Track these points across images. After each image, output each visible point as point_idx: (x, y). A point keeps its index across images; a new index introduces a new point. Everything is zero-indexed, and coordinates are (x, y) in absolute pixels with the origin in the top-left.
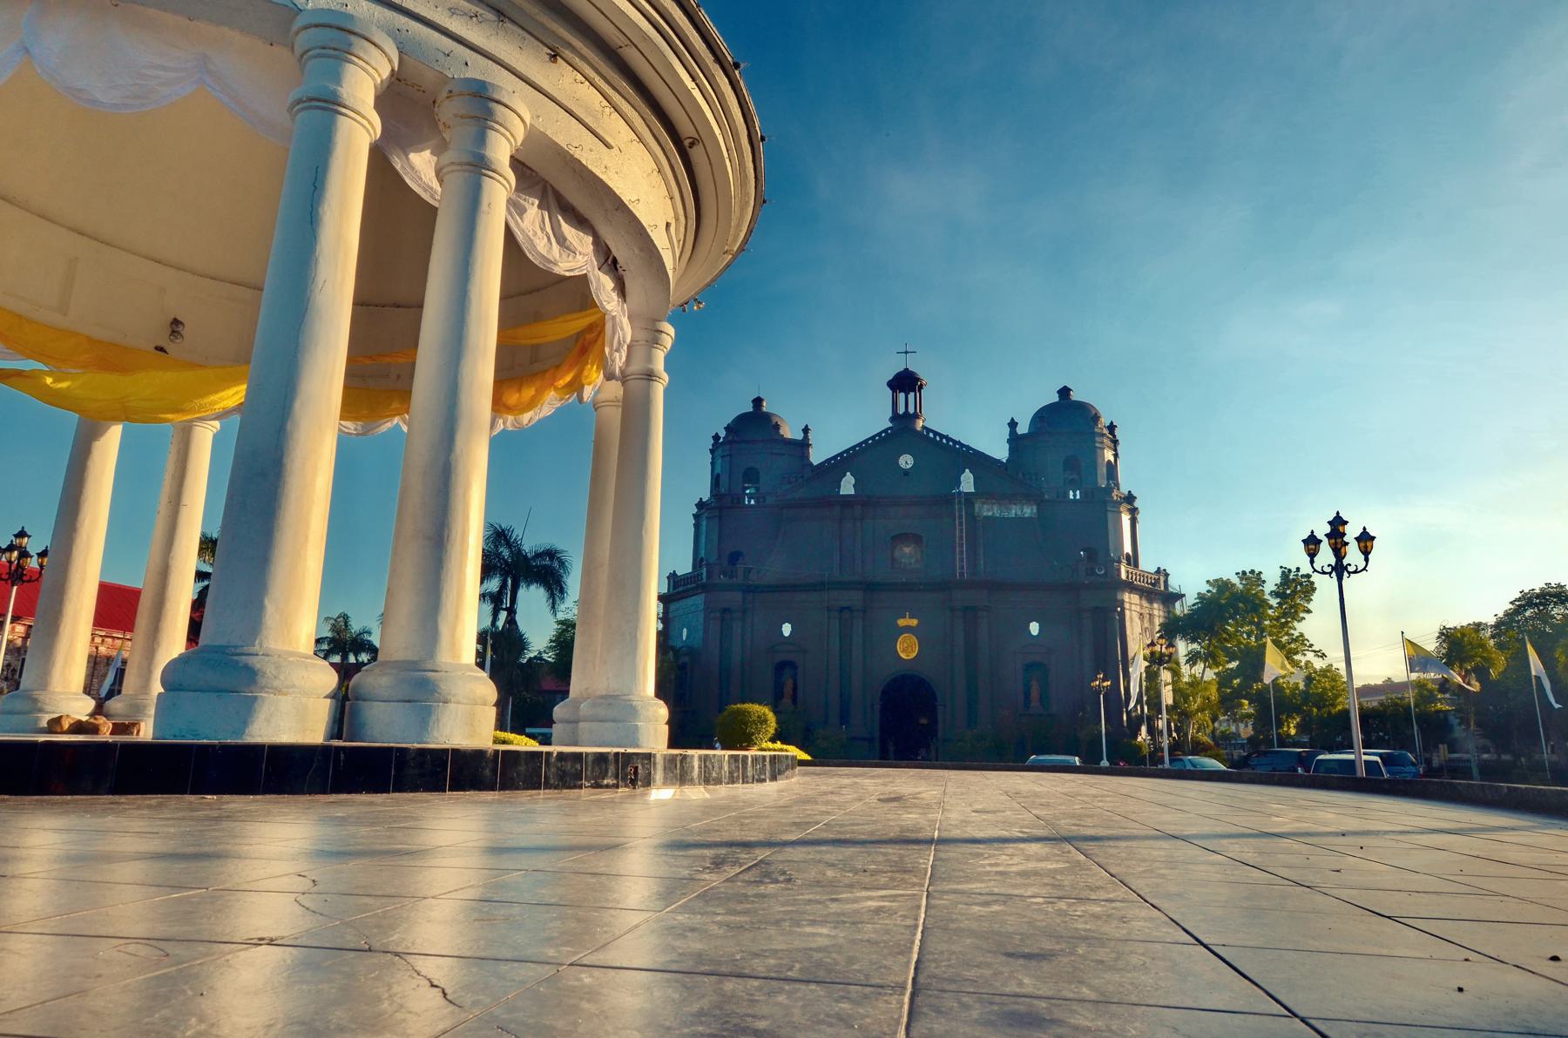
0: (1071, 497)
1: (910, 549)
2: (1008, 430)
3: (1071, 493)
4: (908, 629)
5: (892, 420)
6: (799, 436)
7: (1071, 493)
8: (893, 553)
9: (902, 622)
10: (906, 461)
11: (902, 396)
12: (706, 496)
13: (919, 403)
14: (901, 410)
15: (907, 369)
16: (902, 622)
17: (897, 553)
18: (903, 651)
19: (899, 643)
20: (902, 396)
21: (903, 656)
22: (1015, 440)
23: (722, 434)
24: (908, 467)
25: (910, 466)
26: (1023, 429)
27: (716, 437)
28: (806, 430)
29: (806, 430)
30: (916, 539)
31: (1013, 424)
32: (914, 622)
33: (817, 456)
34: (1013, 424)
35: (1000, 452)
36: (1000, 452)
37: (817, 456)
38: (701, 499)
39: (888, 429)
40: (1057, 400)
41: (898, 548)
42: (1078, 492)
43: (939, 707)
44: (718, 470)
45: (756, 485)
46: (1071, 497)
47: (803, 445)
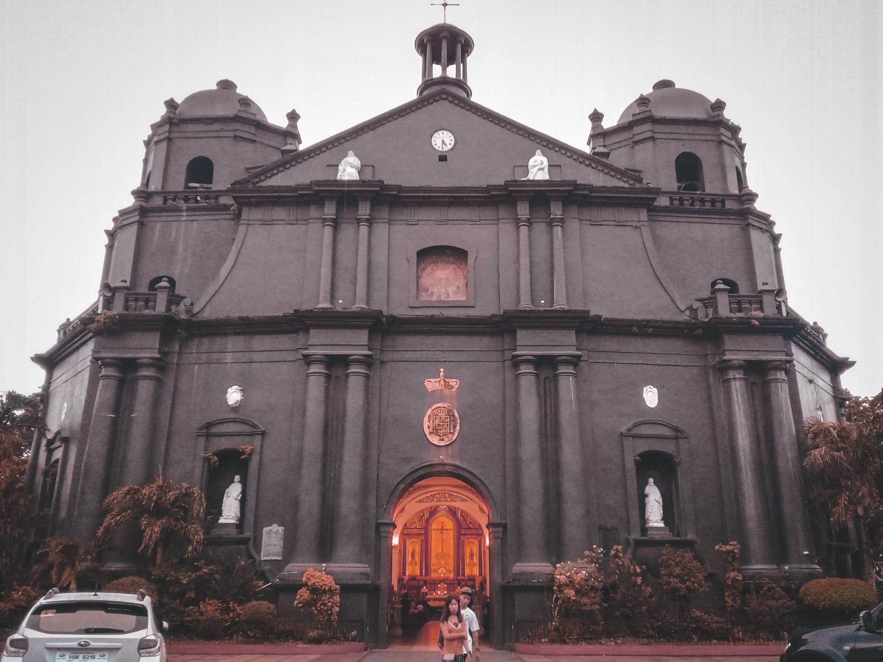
1: (447, 272)
2: (589, 125)
4: (437, 396)
5: (422, 90)
6: (283, 123)
8: (418, 278)
9: (432, 385)
10: (443, 140)
16: (432, 385)
17: (426, 281)
18: (435, 431)
19: (426, 419)
21: (435, 440)
22: (598, 135)
24: (446, 149)
25: (450, 147)
26: (609, 122)
28: (293, 117)
29: (293, 117)
30: (457, 255)
31: (596, 117)
32: (454, 383)
34: (596, 117)
41: (428, 270)
45: (209, 186)
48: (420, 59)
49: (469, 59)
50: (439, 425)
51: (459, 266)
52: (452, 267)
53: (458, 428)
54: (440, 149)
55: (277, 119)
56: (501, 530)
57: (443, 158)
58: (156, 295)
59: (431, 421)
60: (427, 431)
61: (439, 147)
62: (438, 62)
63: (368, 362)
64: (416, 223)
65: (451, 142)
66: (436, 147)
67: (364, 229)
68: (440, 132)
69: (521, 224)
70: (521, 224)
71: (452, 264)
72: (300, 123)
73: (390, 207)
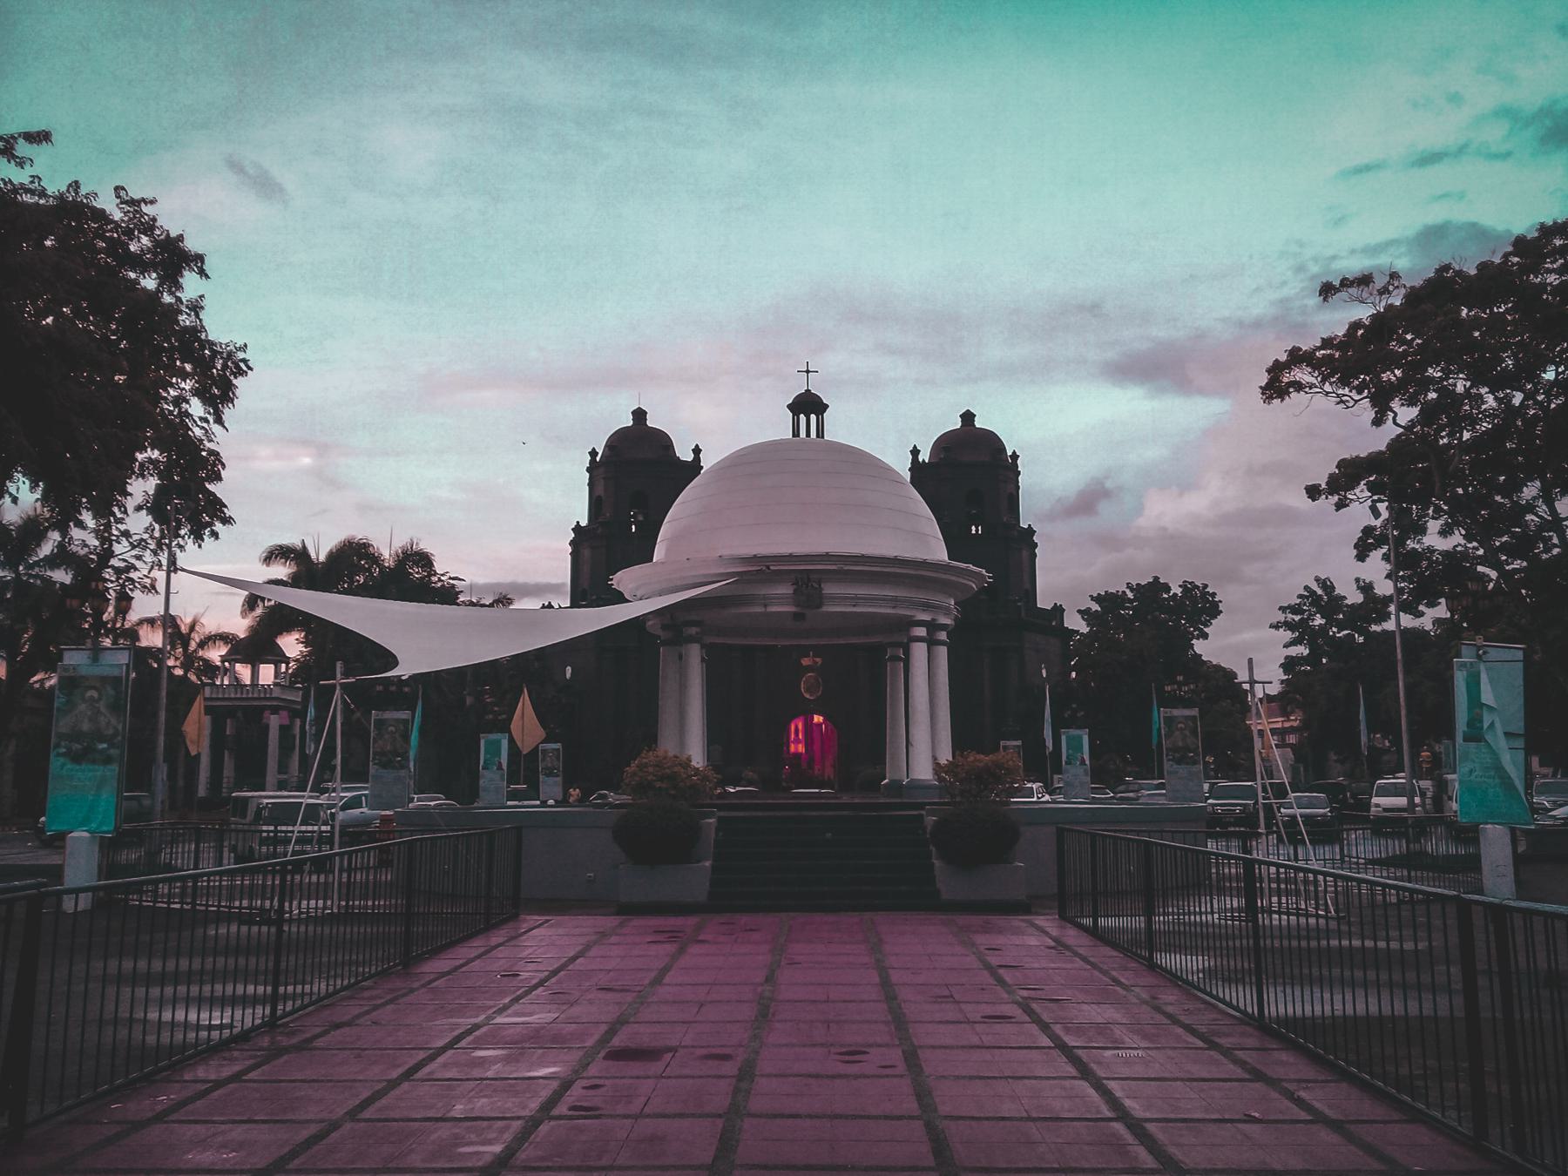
3: (973, 528)
6: (689, 457)
7: (973, 528)
12: (584, 523)
15: (808, 391)
18: (807, 690)
26: (924, 456)
27: (593, 453)
28: (697, 451)
29: (697, 451)
31: (915, 452)
32: (818, 660)
34: (915, 452)
38: (578, 522)
42: (980, 528)
44: (600, 491)
53: (821, 688)
60: (803, 690)
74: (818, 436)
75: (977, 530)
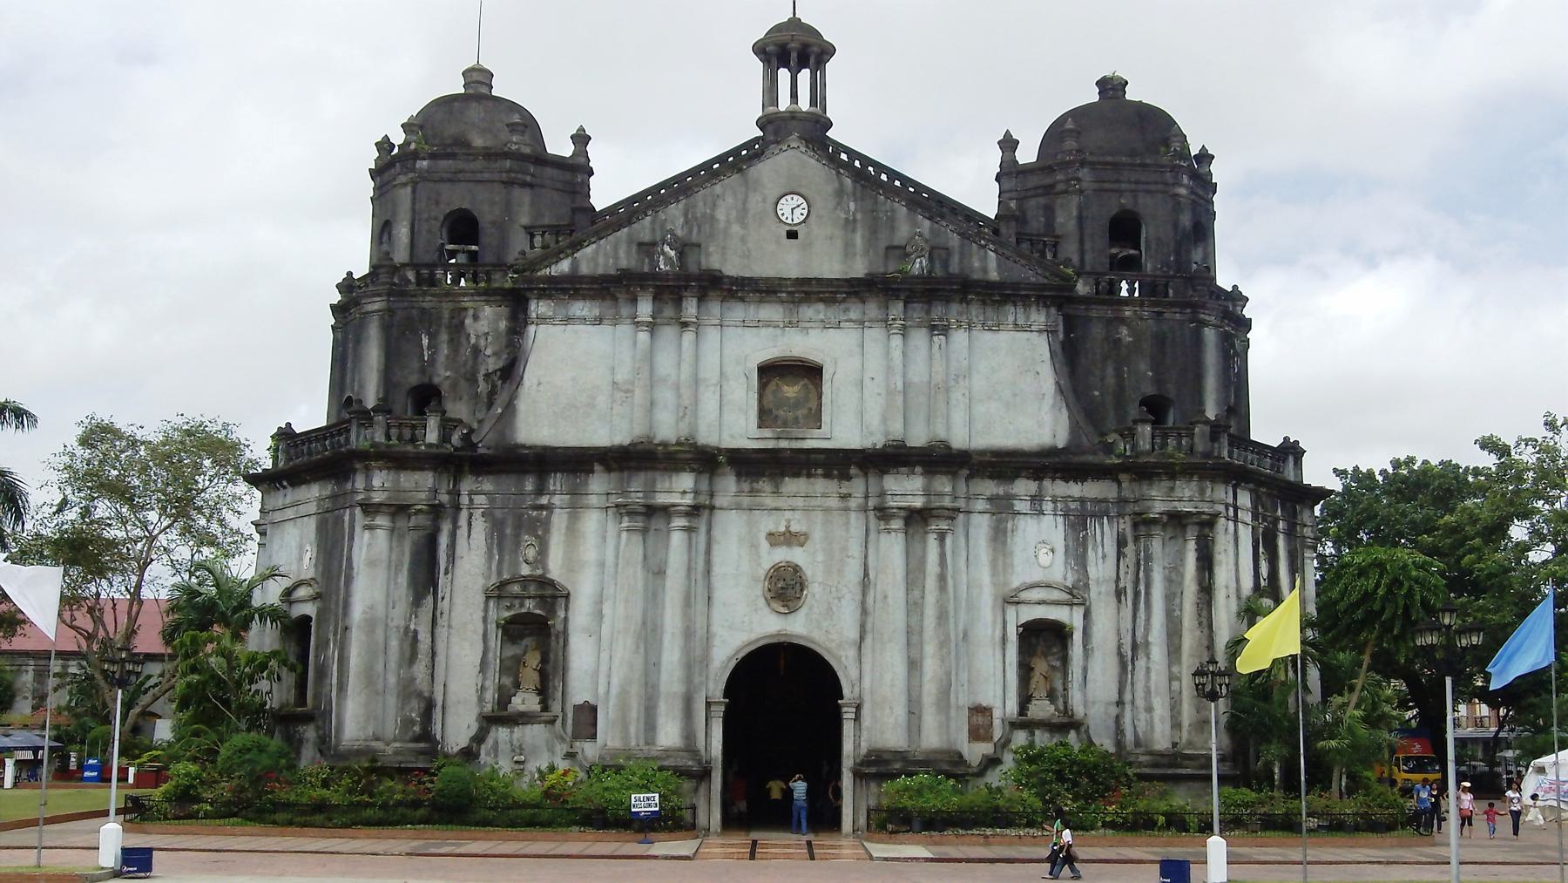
0: (1124, 293)
1: (796, 388)
3: (1124, 285)
5: (761, 124)
7: (1124, 285)
11: (784, 75)
13: (818, 96)
14: (784, 103)
20: (784, 75)
23: (398, 138)
26: (1027, 154)
28: (581, 139)
29: (581, 139)
33: (604, 193)
35: (986, 201)
36: (986, 201)
37: (604, 193)
39: (756, 140)
40: (1096, 98)
43: (844, 709)
46: (1124, 293)
47: (577, 170)
48: (758, 65)
49: (830, 66)
50: (782, 588)
51: (811, 381)
52: (802, 383)
54: (789, 221)
55: (559, 145)
56: (854, 710)
57: (792, 235)
58: (426, 420)
59: (773, 584)
61: (787, 218)
62: (786, 65)
63: (694, 511)
64: (757, 325)
65: (803, 212)
66: (783, 218)
67: (688, 337)
68: (789, 197)
69: (892, 332)
70: (892, 332)
71: (803, 377)
72: (591, 148)
73: (722, 301)
74: (813, 102)
75: (1131, 291)
